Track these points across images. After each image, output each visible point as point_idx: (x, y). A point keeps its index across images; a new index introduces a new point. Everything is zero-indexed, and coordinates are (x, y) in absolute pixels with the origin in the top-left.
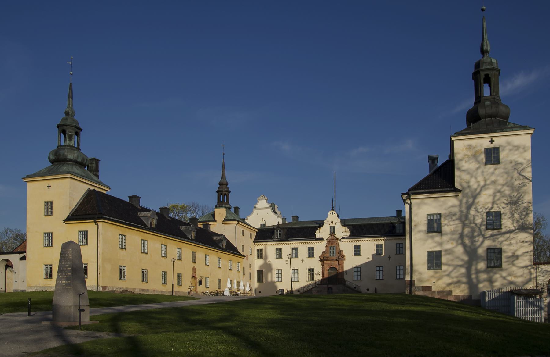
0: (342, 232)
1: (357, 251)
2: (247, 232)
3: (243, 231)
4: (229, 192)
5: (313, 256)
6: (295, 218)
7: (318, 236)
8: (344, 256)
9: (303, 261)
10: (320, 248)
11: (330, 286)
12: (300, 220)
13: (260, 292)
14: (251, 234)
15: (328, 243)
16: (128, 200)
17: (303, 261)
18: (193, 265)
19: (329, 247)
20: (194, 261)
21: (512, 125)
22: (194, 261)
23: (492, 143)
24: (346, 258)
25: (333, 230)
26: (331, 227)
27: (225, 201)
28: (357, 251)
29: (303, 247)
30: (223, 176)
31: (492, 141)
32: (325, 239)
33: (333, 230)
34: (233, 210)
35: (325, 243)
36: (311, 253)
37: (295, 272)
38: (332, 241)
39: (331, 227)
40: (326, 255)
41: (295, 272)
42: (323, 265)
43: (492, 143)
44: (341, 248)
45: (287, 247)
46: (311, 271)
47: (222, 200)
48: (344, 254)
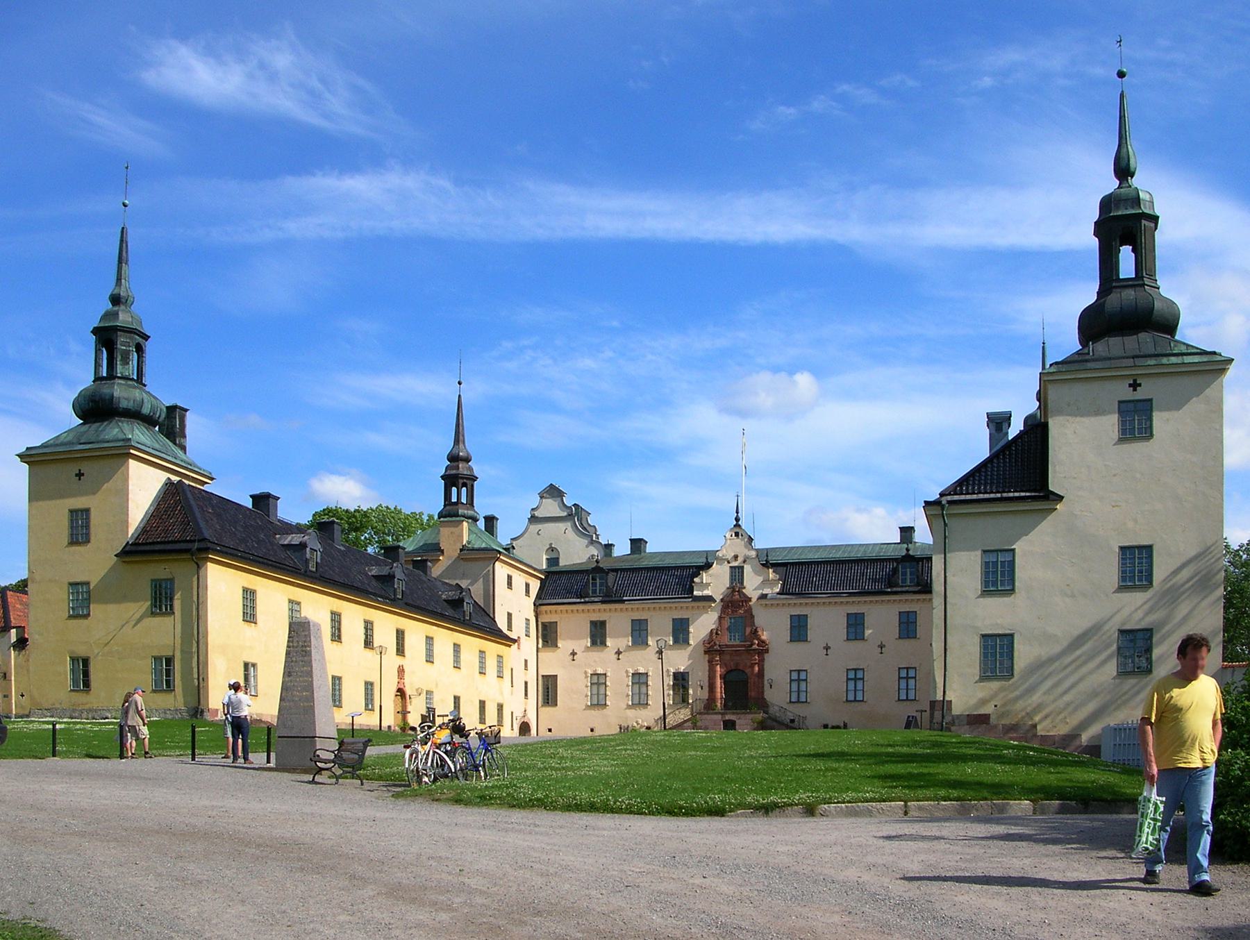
1: (799, 629)
2: (519, 579)
3: (510, 578)
4: (474, 479)
5: (686, 642)
6: (637, 544)
11: (727, 717)
12: (650, 549)
13: (550, 730)
14: (527, 585)
16: (249, 503)
18: (399, 661)
20: (400, 651)
21: (1183, 349)
22: (400, 651)
23: (1135, 390)
25: (737, 574)
27: (464, 500)
28: (799, 629)
29: (660, 620)
30: (458, 438)
31: (1135, 386)
33: (737, 574)
34: (481, 524)
38: (735, 603)
43: (1135, 390)
44: (758, 622)
45: (618, 618)
46: (681, 680)
47: (454, 499)
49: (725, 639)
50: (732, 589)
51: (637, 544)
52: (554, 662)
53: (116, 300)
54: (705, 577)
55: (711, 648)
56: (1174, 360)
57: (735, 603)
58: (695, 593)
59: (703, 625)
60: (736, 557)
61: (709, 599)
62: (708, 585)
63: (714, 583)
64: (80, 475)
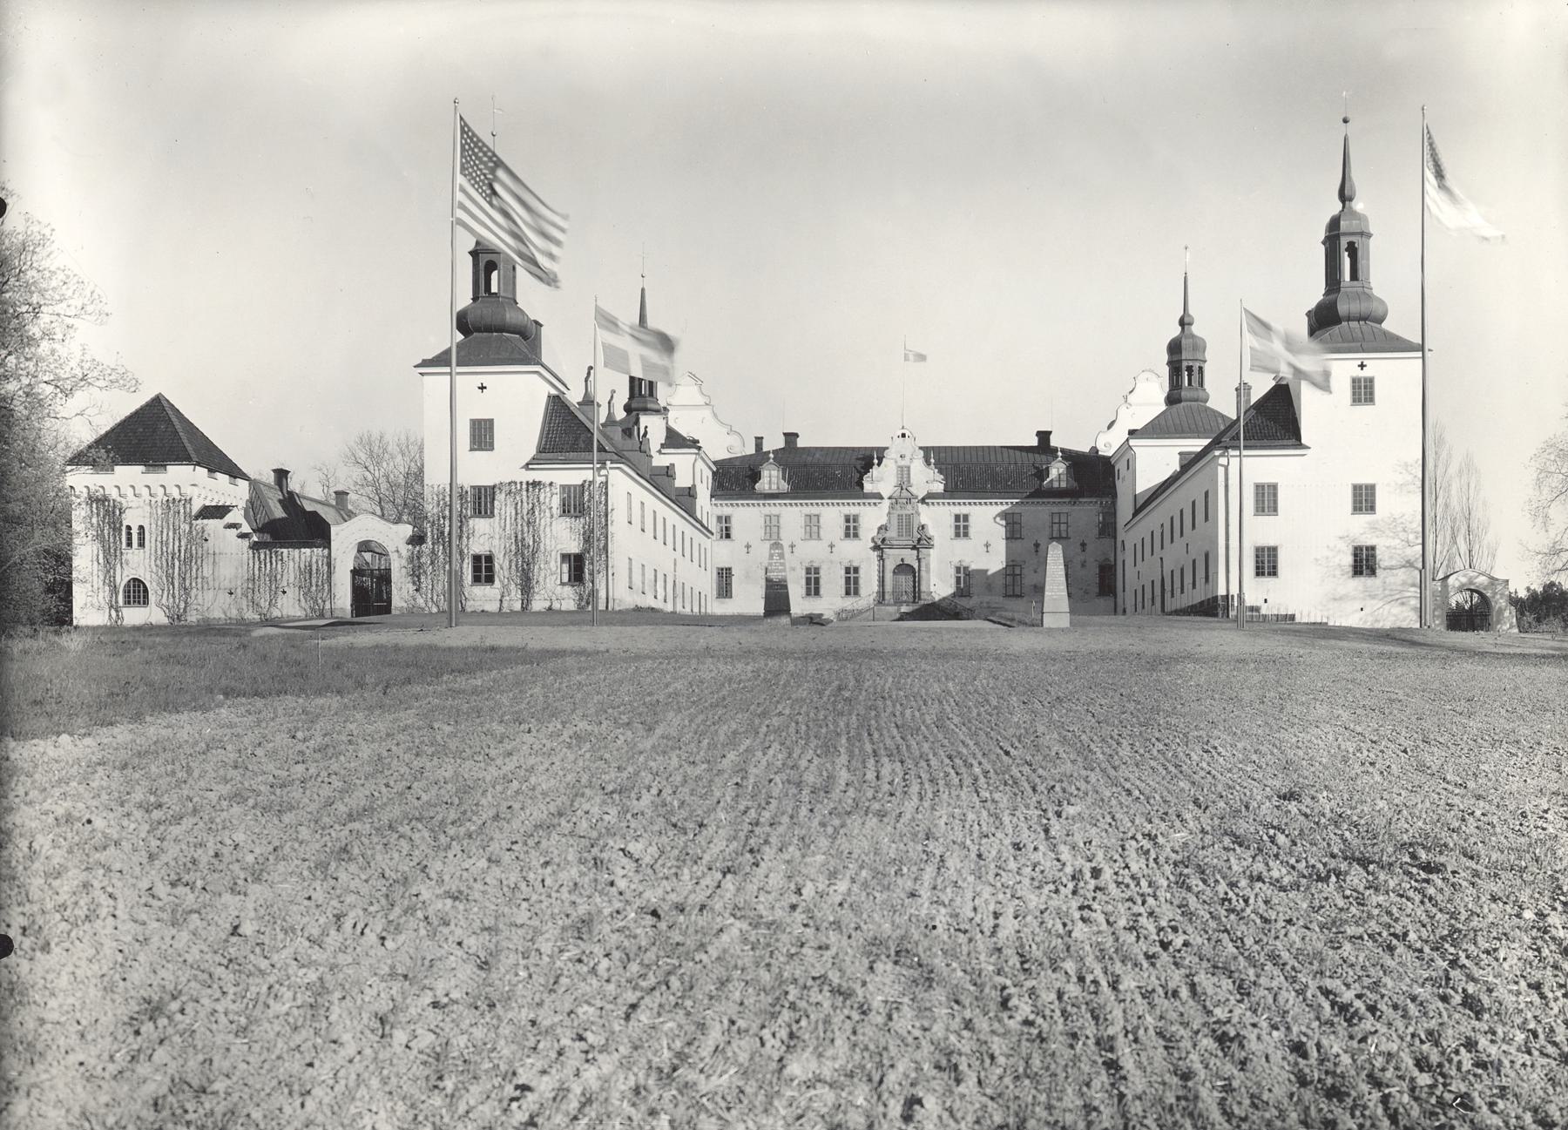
1: (961, 528)
6: (791, 437)
7: (868, 487)
9: (832, 546)
10: (873, 518)
12: (801, 443)
15: (892, 507)
17: (832, 546)
19: (895, 521)
24: (936, 542)
28: (961, 528)
29: (832, 513)
31: (1362, 366)
32: (885, 495)
33: (904, 472)
35: (886, 503)
36: (851, 529)
40: (887, 535)
42: (881, 558)
48: (931, 531)
51: (791, 437)
61: (879, 496)
63: (881, 480)
64: (482, 388)
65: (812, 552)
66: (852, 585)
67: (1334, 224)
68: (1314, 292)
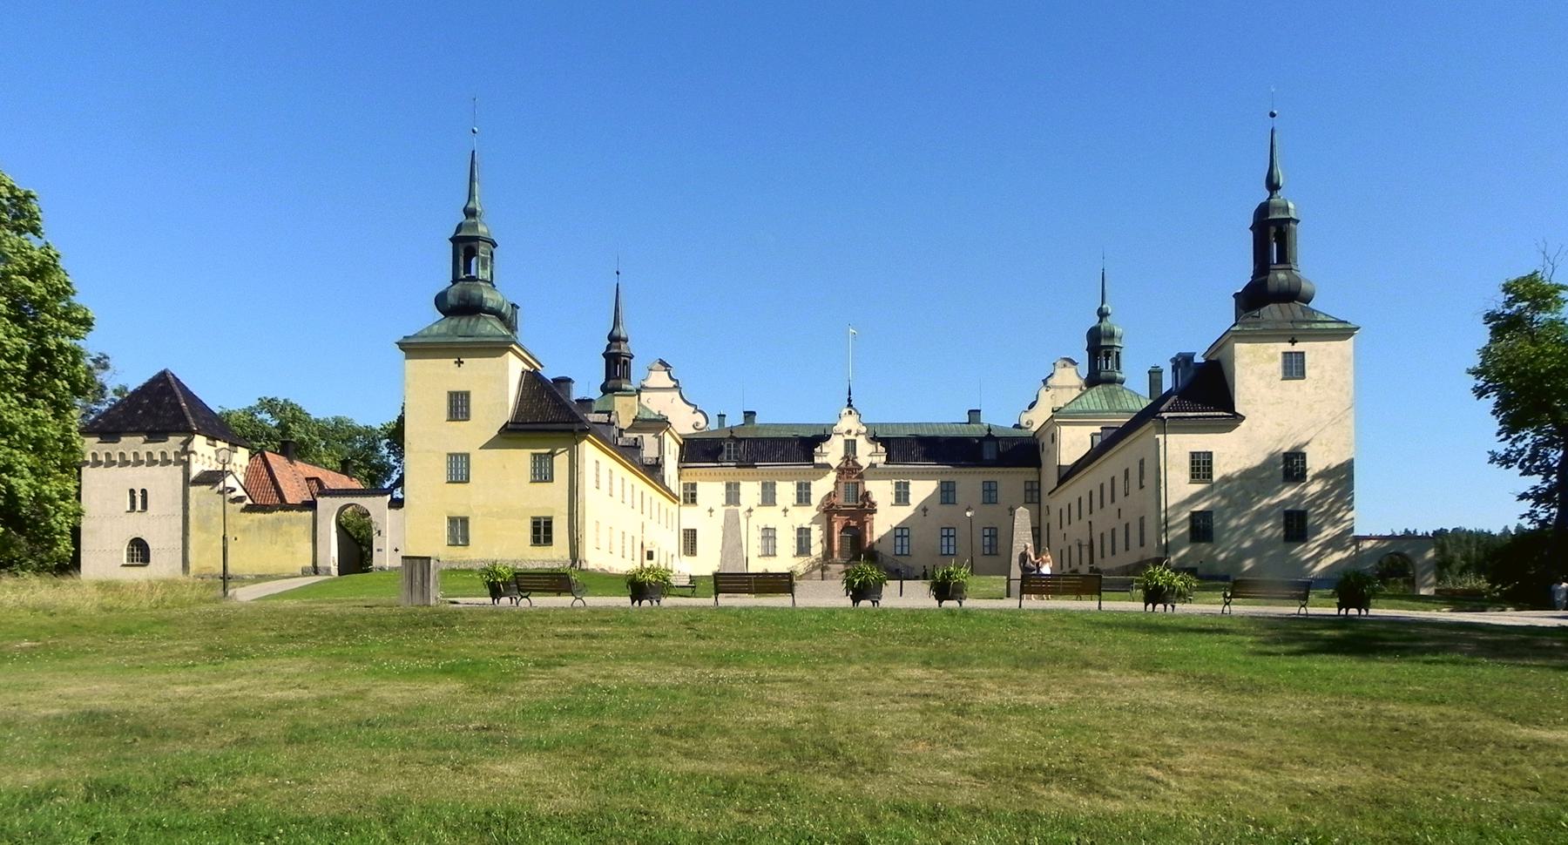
0: (866, 454)
1: (902, 497)
5: (808, 502)
6: (749, 415)
8: (873, 504)
9: (785, 510)
12: (758, 420)
15: (839, 477)
17: (785, 510)
19: (841, 487)
25: (850, 446)
26: (847, 441)
28: (902, 497)
33: (850, 446)
35: (832, 476)
37: (769, 534)
38: (850, 470)
39: (847, 441)
40: (835, 501)
41: (769, 534)
46: (803, 535)
48: (874, 499)
49: (839, 500)
50: (846, 457)
51: (749, 415)
52: (691, 517)
53: (470, 213)
54: (826, 447)
55: (829, 510)
56: (1320, 326)
57: (850, 470)
58: (817, 460)
59: (823, 487)
60: (849, 432)
61: (827, 466)
62: (826, 455)
63: (832, 452)
65: (768, 516)
66: (803, 548)
67: (1263, 210)
68: (1243, 275)
